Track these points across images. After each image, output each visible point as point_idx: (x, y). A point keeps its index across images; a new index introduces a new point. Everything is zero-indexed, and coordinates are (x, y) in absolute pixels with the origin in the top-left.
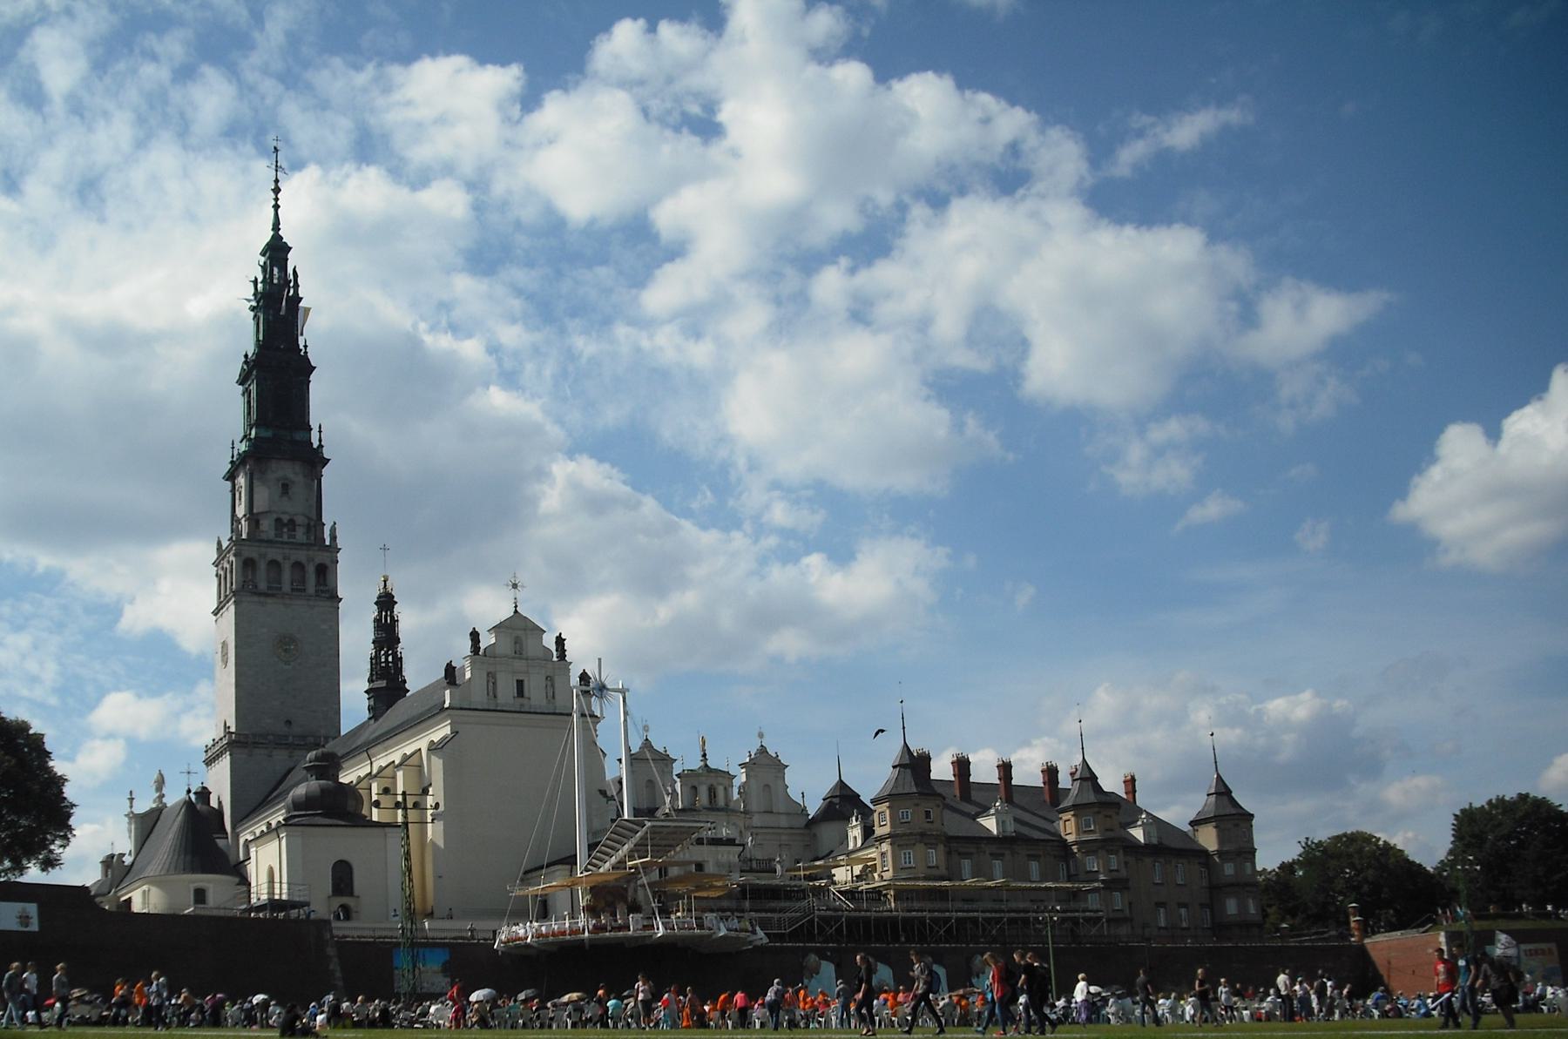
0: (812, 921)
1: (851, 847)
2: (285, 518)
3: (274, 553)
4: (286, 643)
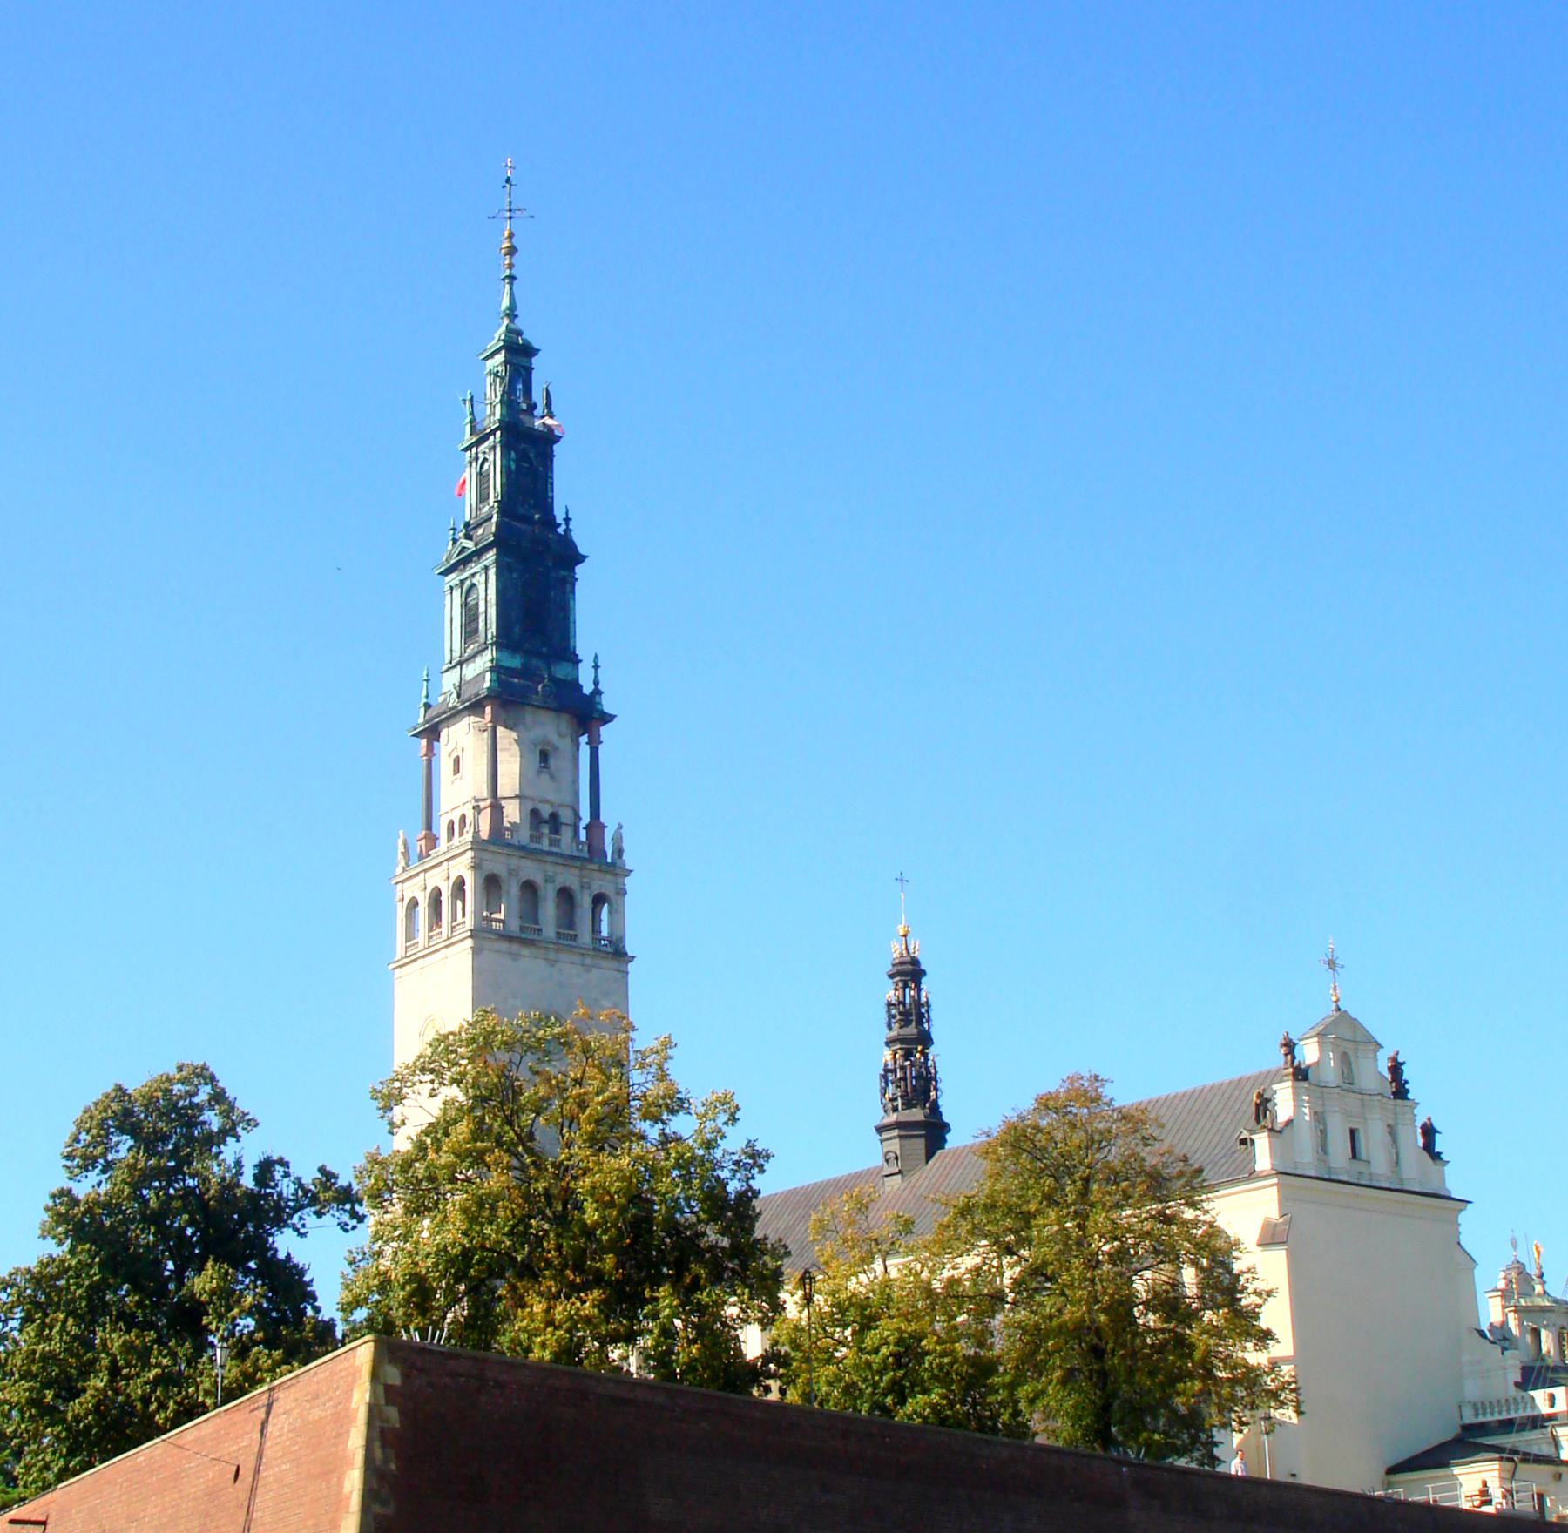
2: (546, 811)
3: (530, 870)
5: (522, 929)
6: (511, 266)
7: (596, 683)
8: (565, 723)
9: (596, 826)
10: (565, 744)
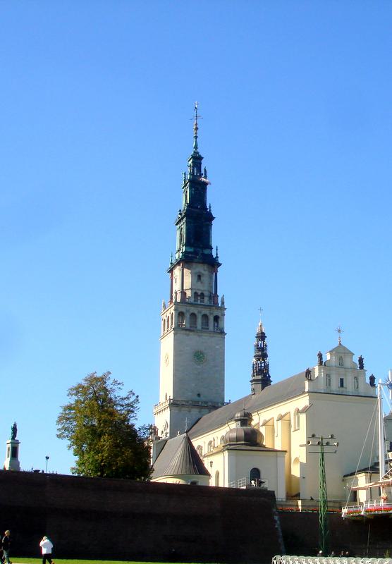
2: (199, 293)
3: (193, 310)
4: (199, 356)
5: (191, 327)
6: (196, 133)
7: (217, 254)
8: (206, 267)
9: (216, 296)
10: (206, 273)
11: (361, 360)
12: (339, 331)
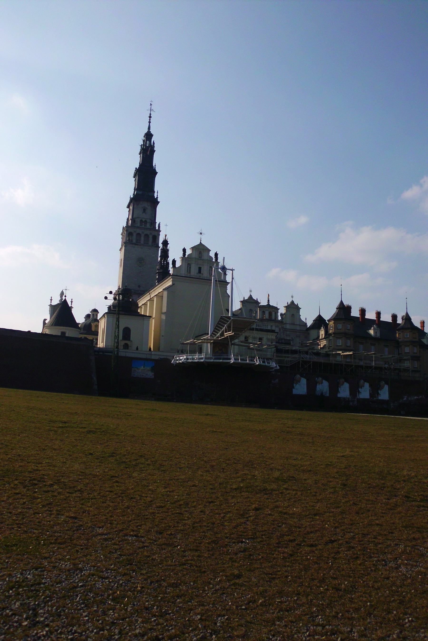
0: (299, 362)
1: (320, 338)
2: (144, 220)
3: (138, 231)
4: (140, 261)
5: (136, 242)
11: (216, 255)
12: (201, 234)
